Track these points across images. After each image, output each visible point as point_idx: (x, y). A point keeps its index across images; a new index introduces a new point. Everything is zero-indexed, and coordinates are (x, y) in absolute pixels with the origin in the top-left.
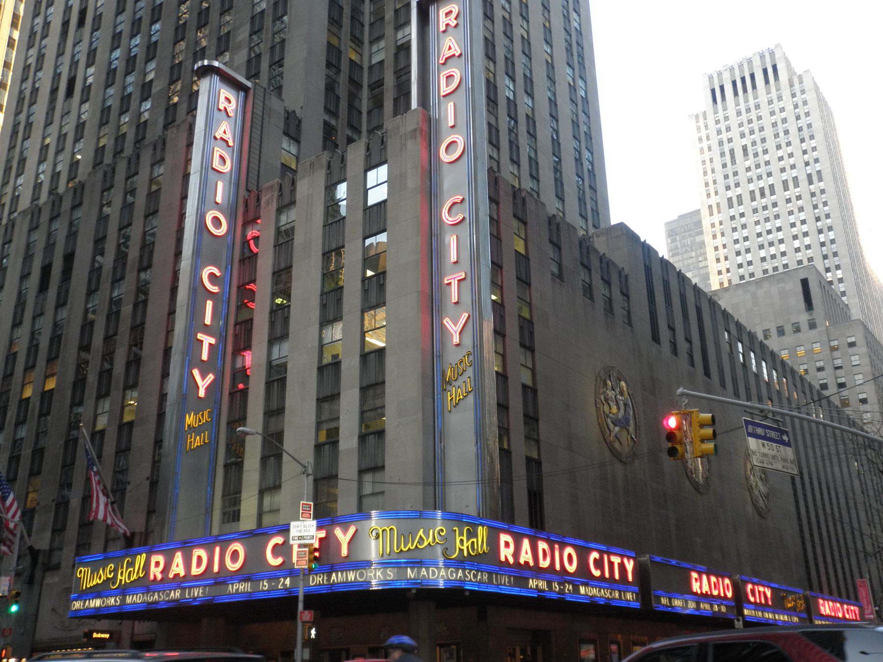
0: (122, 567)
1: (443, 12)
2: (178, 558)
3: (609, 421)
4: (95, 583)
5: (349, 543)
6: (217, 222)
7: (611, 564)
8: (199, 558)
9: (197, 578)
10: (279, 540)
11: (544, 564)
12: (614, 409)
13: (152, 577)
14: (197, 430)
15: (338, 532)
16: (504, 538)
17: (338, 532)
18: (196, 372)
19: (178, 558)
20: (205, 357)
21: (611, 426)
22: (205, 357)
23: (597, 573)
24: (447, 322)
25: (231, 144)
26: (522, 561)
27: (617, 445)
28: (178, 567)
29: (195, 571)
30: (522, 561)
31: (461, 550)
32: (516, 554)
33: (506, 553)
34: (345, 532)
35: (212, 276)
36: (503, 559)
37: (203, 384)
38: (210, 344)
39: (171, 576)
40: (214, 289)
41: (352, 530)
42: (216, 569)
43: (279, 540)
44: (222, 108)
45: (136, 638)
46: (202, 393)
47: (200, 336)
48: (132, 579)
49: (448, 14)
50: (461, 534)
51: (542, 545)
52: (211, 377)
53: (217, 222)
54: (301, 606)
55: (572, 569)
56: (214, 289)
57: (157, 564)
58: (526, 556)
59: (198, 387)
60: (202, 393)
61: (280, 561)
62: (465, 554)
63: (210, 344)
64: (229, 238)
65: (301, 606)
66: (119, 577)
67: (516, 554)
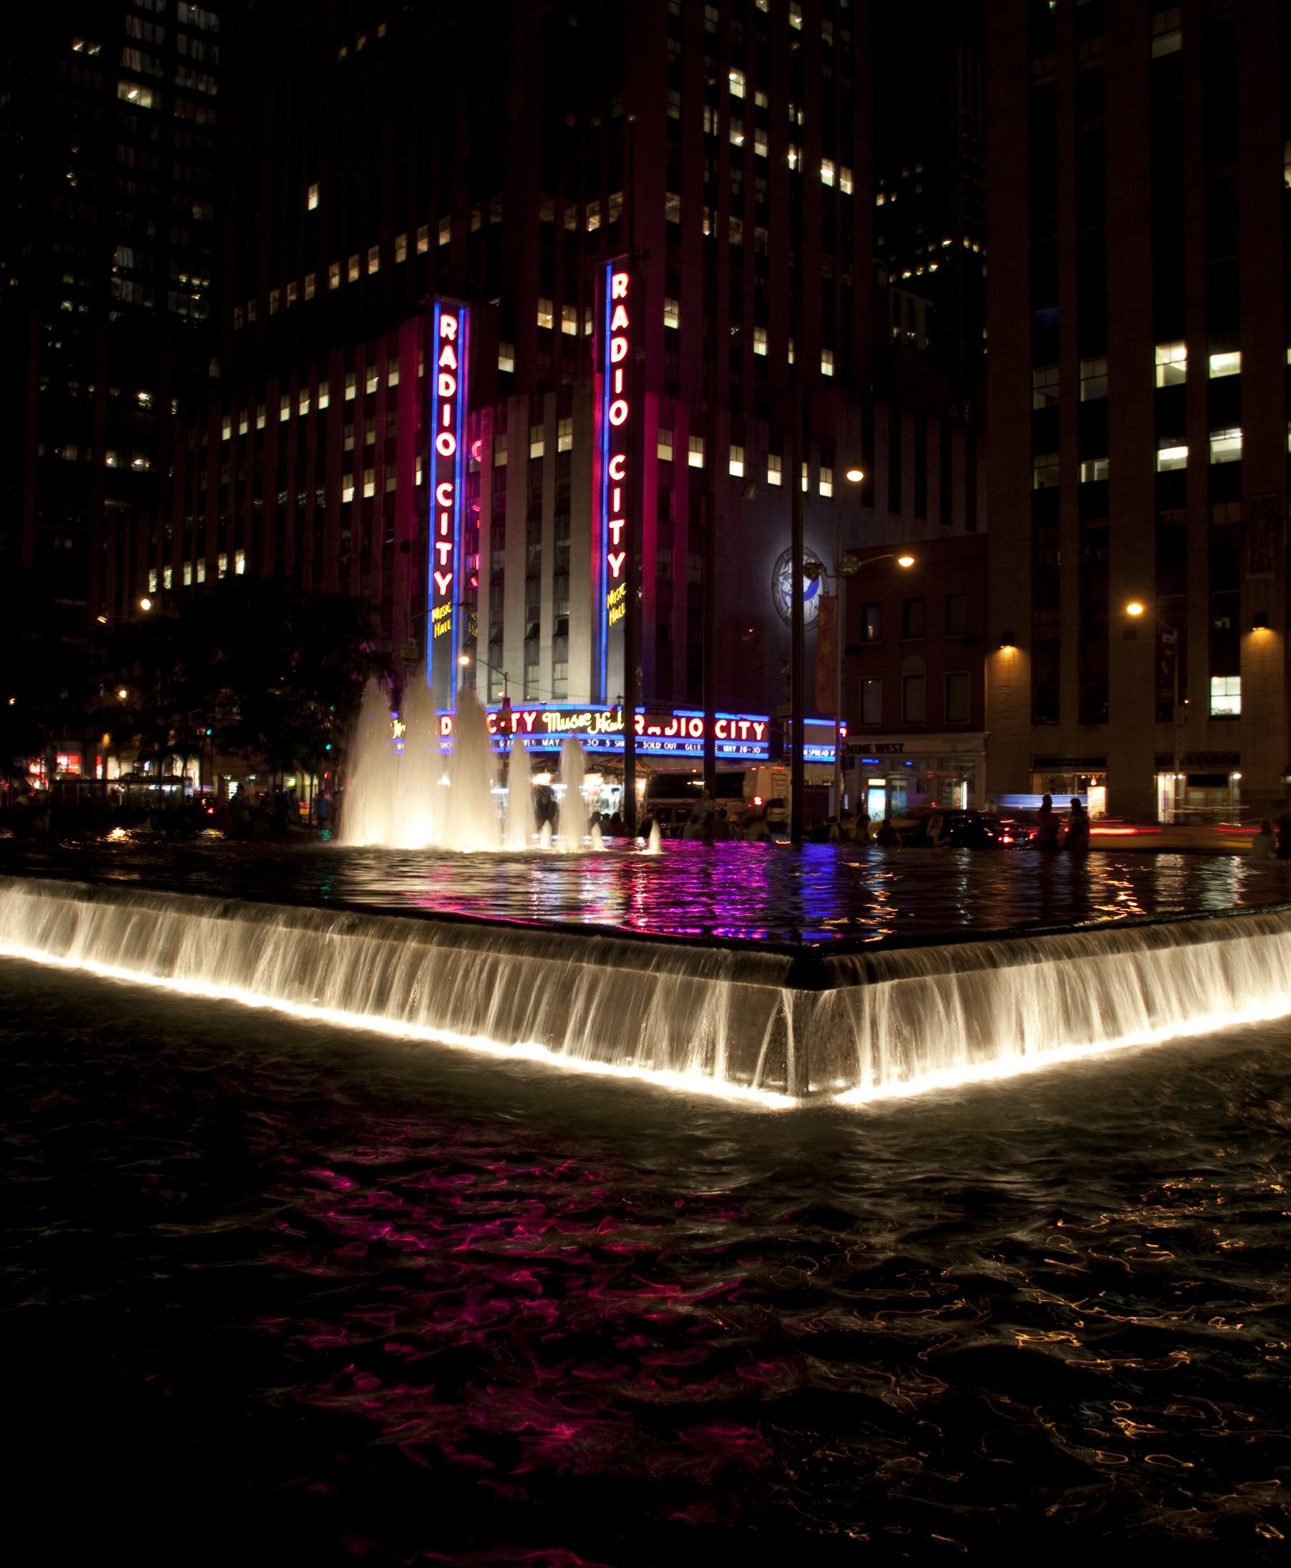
6: (446, 444)
14: (443, 621)
15: (526, 715)
18: (438, 575)
20: (443, 561)
22: (443, 561)
25: (453, 367)
37: (443, 583)
40: (447, 503)
41: (534, 714)
46: (443, 592)
52: (449, 577)
53: (446, 444)
56: (447, 503)
60: (443, 592)
64: (458, 455)
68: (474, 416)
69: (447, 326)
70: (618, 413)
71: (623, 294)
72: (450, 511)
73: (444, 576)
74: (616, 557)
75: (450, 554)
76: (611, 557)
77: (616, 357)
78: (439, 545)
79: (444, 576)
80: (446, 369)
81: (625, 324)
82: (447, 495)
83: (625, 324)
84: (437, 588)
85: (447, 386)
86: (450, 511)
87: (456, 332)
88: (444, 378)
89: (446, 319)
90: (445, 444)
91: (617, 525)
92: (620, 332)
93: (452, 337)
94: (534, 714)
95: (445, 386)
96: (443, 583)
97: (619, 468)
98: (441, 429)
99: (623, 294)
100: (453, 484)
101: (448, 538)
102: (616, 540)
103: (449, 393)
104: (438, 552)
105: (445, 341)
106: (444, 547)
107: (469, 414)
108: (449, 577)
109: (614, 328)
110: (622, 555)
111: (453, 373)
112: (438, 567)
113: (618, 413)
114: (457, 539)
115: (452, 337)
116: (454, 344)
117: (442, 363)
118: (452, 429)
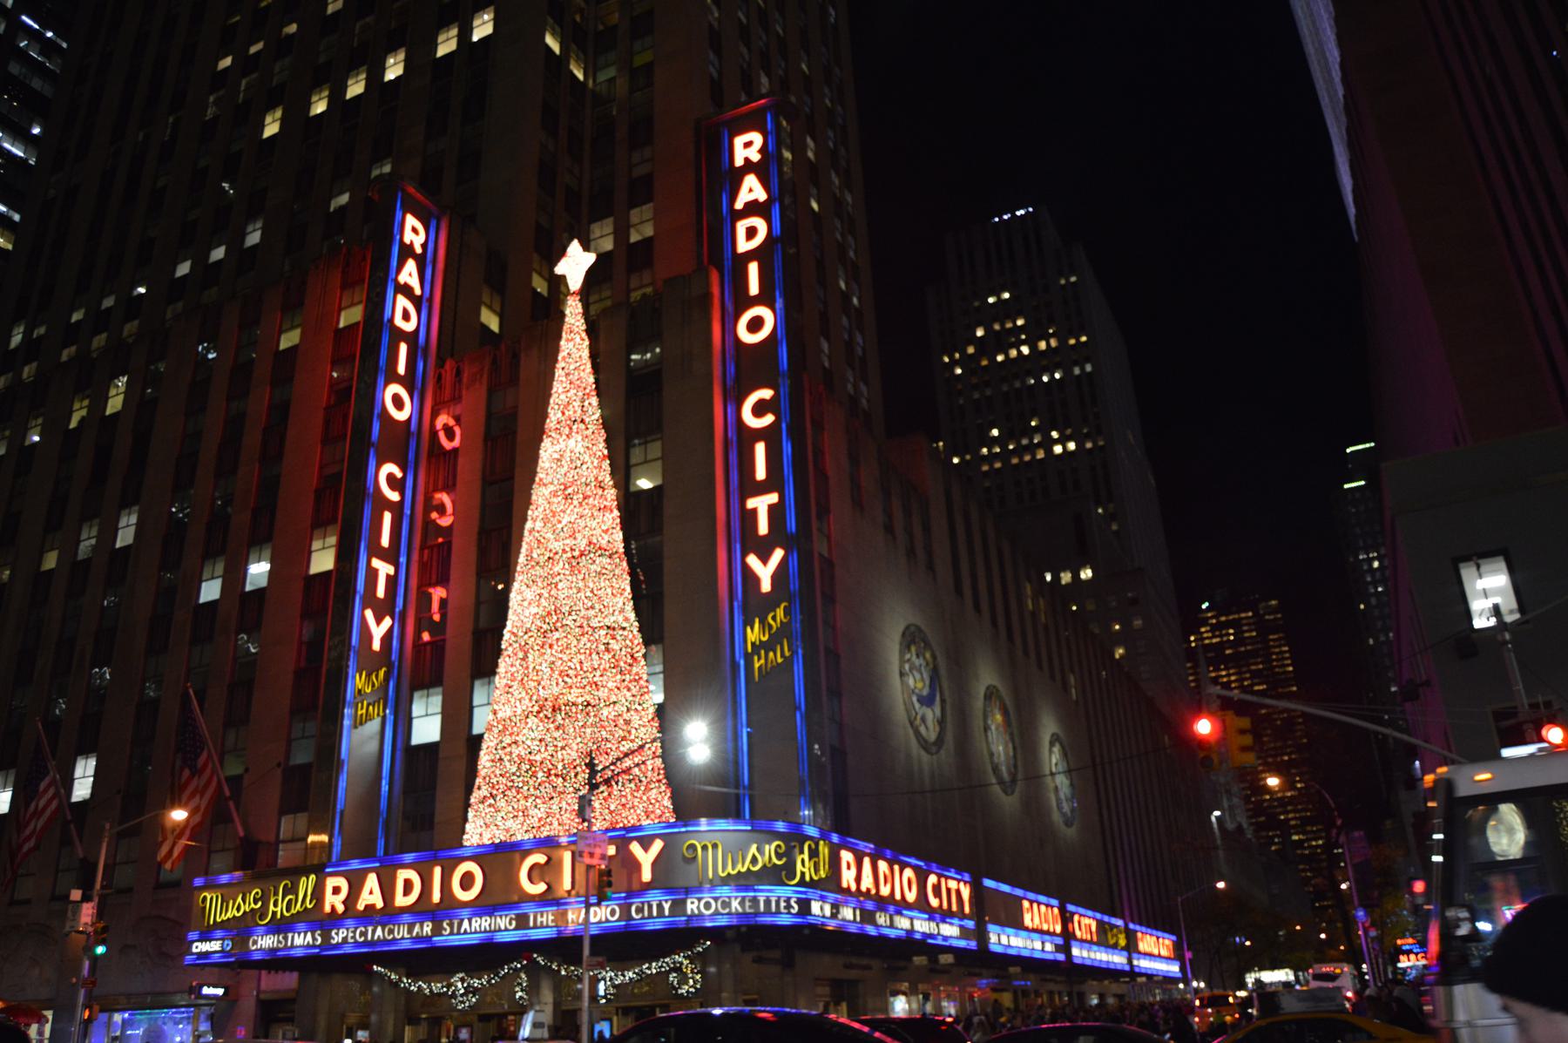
0: (276, 894)
1: (739, 141)
2: (372, 881)
3: (914, 699)
4: (229, 915)
5: (654, 864)
7: (949, 890)
8: (408, 885)
9: (404, 910)
10: (540, 858)
11: (885, 891)
12: (920, 685)
13: (328, 909)
15: (635, 848)
16: (846, 856)
17: (635, 848)
18: (369, 614)
19: (372, 881)
20: (381, 593)
21: (917, 705)
22: (381, 593)
23: (934, 902)
24: (753, 561)
25: (418, 291)
26: (864, 889)
27: (922, 729)
28: (371, 894)
29: (401, 901)
30: (864, 889)
31: (803, 874)
32: (858, 879)
33: (848, 877)
34: (646, 849)
35: (391, 478)
36: (845, 885)
37: (378, 631)
38: (388, 576)
39: (361, 906)
40: (394, 496)
41: (658, 845)
42: (436, 897)
43: (540, 858)
44: (407, 240)
45: (262, 996)
46: (376, 646)
47: (376, 563)
48: (293, 911)
49: (748, 145)
50: (802, 852)
51: (883, 866)
54: (586, 951)
55: (911, 897)
56: (394, 496)
57: (336, 890)
58: (867, 882)
59: (370, 638)
60: (376, 646)
61: (540, 888)
62: (807, 878)
63: (388, 576)
65: (586, 951)
66: (272, 907)
67: (858, 879)
68: (449, 364)
69: (413, 232)
70: (756, 324)
71: (756, 157)
72: (397, 509)
73: (379, 621)
74: (765, 560)
75: (392, 581)
76: (753, 561)
77: (743, 246)
78: (376, 563)
79: (379, 621)
80: (406, 290)
81: (761, 195)
82: (391, 478)
83: (761, 195)
84: (367, 635)
85: (406, 316)
86: (397, 509)
87: (424, 246)
88: (402, 302)
89: (411, 221)
90: (397, 403)
91: (761, 504)
92: (753, 208)
93: (419, 250)
94: (658, 845)
95: (403, 315)
96: (378, 631)
97: (759, 410)
98: (395, 378)
99: (756, 157)
100: (403, 469)
101: (390, 556)
102: (763, 528)
103: (409, 327)
104: (373, 574)
105: (407, 251)
106: (384, 569)
107: (441, 361)
108: (387, 622)
109: (739, 205)
110: (779, 554)
111: (417, 301)
112: (370, 600)
113: (756, 324)
114: (403, 560)
115: (419, 250)
116: (421, 261)
117: (403, 278)
118: (408, 382)
